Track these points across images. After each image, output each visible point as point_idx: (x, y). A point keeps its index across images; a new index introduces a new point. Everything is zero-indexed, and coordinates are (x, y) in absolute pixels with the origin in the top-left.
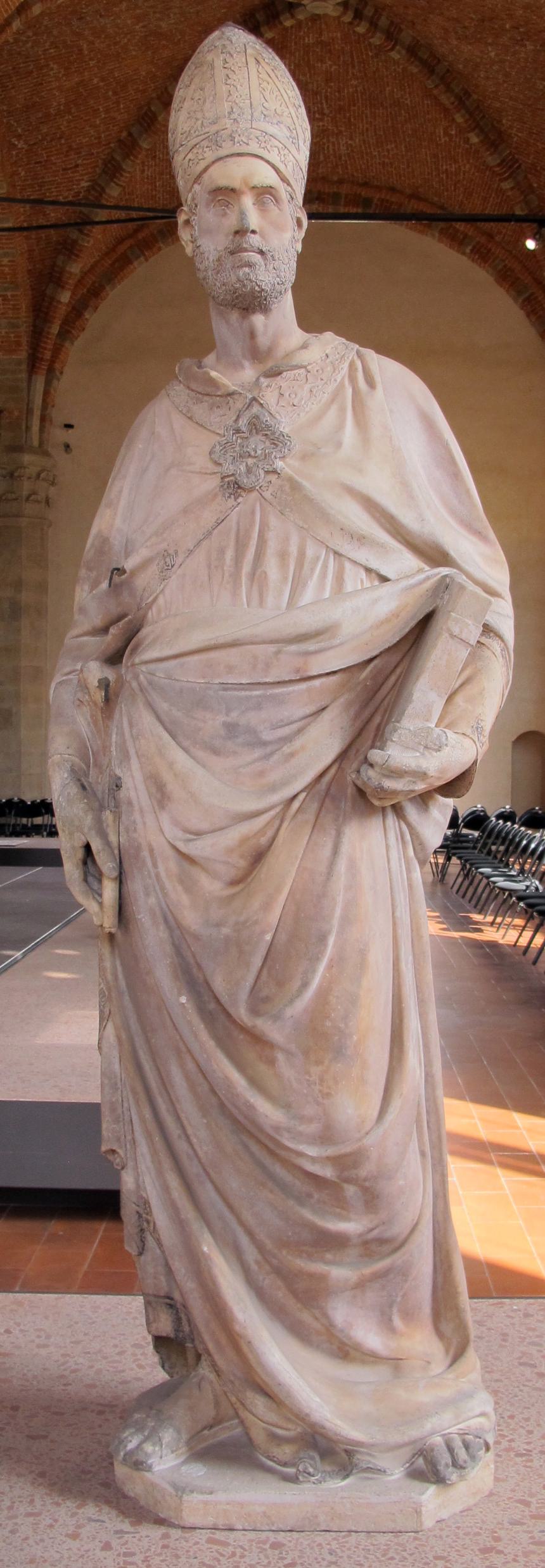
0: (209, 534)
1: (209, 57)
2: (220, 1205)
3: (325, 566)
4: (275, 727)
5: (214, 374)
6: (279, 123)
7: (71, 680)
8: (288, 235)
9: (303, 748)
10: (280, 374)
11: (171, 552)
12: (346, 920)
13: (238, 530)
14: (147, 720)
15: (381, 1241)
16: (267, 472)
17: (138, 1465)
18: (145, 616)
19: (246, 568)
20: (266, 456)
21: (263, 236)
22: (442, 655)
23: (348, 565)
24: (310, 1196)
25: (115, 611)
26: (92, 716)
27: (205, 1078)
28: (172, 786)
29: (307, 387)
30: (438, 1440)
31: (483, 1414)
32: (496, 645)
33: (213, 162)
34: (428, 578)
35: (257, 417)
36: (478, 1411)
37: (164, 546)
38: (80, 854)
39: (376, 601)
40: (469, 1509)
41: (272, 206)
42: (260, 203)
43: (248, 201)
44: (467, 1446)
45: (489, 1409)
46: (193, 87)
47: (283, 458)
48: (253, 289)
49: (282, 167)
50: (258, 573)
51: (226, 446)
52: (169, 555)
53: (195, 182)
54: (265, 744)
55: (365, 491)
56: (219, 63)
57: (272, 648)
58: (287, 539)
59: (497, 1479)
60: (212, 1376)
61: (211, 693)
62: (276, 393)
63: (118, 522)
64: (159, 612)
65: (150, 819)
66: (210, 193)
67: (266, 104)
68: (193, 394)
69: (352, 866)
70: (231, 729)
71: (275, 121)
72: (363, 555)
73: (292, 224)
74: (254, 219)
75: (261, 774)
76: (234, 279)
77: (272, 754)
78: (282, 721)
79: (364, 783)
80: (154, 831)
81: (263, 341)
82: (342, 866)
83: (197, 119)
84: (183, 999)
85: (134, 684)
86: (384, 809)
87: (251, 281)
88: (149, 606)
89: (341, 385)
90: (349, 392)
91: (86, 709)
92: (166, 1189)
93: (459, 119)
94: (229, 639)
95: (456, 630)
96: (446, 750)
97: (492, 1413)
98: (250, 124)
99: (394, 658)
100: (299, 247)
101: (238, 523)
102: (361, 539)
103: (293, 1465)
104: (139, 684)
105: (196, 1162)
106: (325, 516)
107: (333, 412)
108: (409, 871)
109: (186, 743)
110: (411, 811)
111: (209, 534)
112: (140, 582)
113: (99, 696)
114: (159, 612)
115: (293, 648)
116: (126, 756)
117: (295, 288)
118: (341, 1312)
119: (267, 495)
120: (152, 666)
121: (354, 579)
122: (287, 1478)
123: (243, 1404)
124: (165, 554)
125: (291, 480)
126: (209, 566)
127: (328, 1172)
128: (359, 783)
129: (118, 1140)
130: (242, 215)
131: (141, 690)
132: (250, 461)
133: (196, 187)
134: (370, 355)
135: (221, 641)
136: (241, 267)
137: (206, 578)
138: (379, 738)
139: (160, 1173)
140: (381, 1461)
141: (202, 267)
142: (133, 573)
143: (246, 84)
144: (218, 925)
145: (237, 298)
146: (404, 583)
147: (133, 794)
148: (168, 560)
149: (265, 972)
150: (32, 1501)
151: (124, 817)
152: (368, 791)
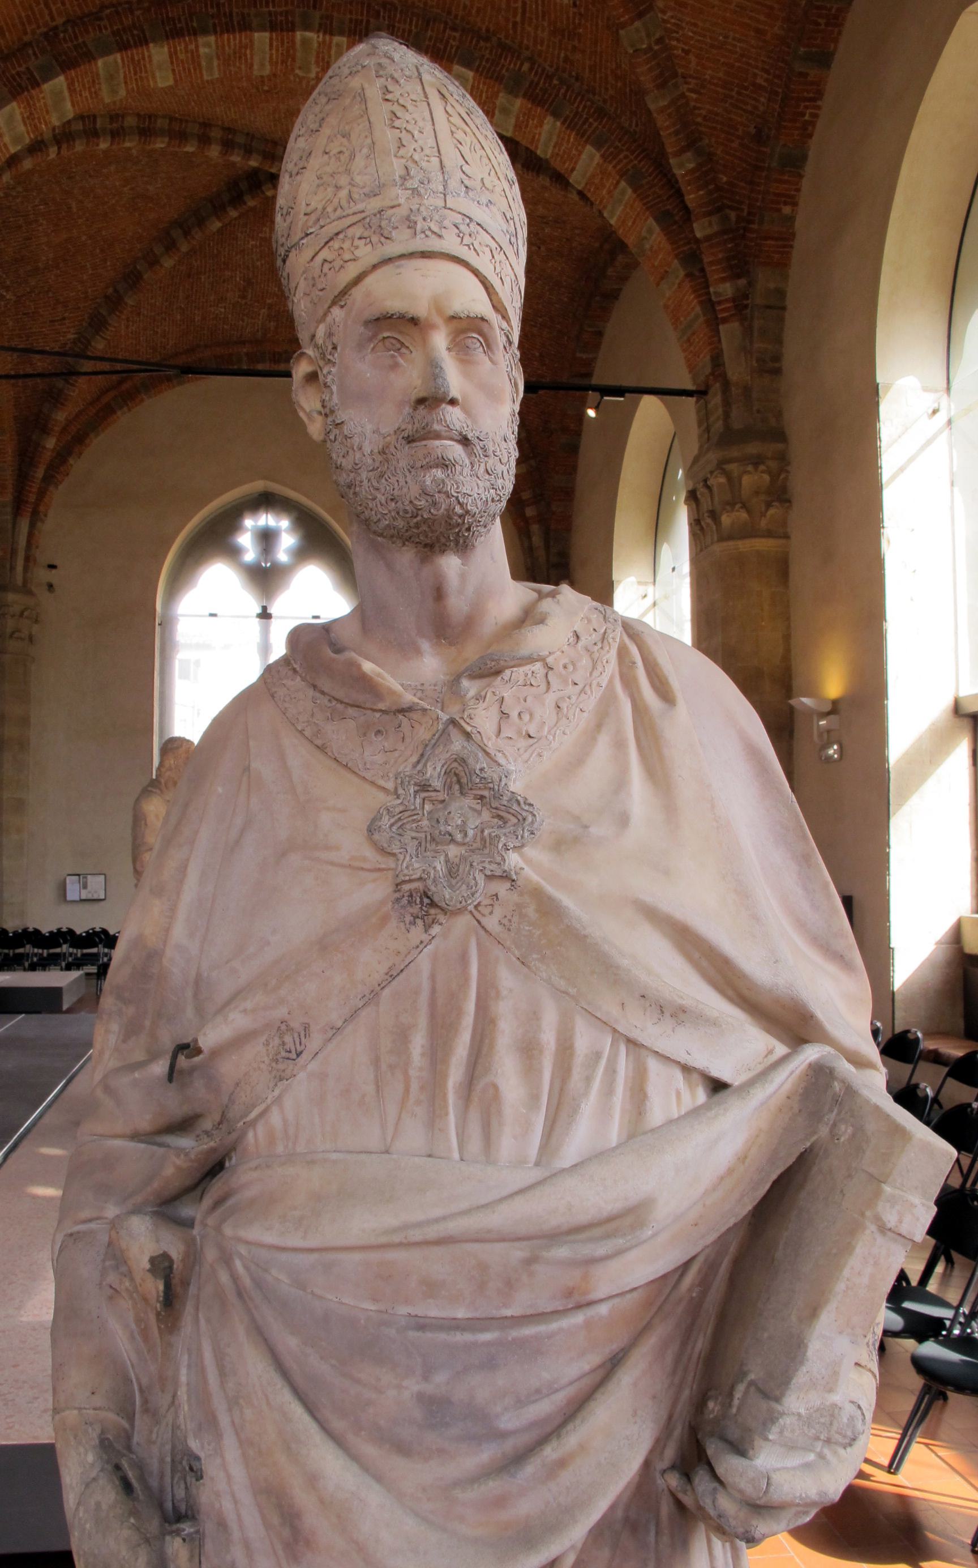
0: (372, 997)
1: (355, 83)
3: (611, 1071)
4: (521, 1403)
7: (91, 1232)
9: (582, 1448)
10: (498, 672)
11: (295, 1024)
13: (433, 991)
16: (490, 878)
20: (486, 844)
21: (467, 411)
23: (653, 1065)
25: (174, 1105)
26: (138, 1321)
28: (313, 1520)
29: (550, 698)
33: (375, 267)
37: (281, 1012)
41: (479, 355)
42: (459, 346)
46: (326, 131)
48: (450, 510)
50: (480, 1086)
52: (289, 1029)
53: (334, 303)
54: (503, 1435)
55: (679, 914)
56: (373, 92)
57: (518, 1253)
58: (534, 1016)
61: (392, 1332)
62: (494, 713)
63: (179, 932)
64: (272, 1140)
66: (367, 323)
67: (465, 168)
68: (325, 700)
70: (436, 1409)
71: (484, 200)
73: (508, 388)
75: (500, 1502)
76: (414, 490)
78: (538, 1391)
81: (457, 604)
83: (338, 188)
85: (224, 1277)
87: (448, 495)
91: (125, 1304)
95: (891, 1219)
101: (433, 977)
102: (678, 1014)
104: (235, 1278)
106: (609, 971)
109: (338, 1425)
111: (372, 997)
112: (229, 1069)
114: (272, 1140)
116: (210, 1423)
119: (492, 923)
124: (283, 1027)
125: (538, 894)
126: (376, 1062)
130: (433, 369)
131: (240, 1294)
132: (453, 851)
133: (337, 312)
136: (428, 467)
137: (370, 1089)
141: (346, 463)
142: (216, 1053)
143: (429, 127)
145: (417, 526)
147: (227, 1505)
148: (288, 1039)
151: (209, 1546)
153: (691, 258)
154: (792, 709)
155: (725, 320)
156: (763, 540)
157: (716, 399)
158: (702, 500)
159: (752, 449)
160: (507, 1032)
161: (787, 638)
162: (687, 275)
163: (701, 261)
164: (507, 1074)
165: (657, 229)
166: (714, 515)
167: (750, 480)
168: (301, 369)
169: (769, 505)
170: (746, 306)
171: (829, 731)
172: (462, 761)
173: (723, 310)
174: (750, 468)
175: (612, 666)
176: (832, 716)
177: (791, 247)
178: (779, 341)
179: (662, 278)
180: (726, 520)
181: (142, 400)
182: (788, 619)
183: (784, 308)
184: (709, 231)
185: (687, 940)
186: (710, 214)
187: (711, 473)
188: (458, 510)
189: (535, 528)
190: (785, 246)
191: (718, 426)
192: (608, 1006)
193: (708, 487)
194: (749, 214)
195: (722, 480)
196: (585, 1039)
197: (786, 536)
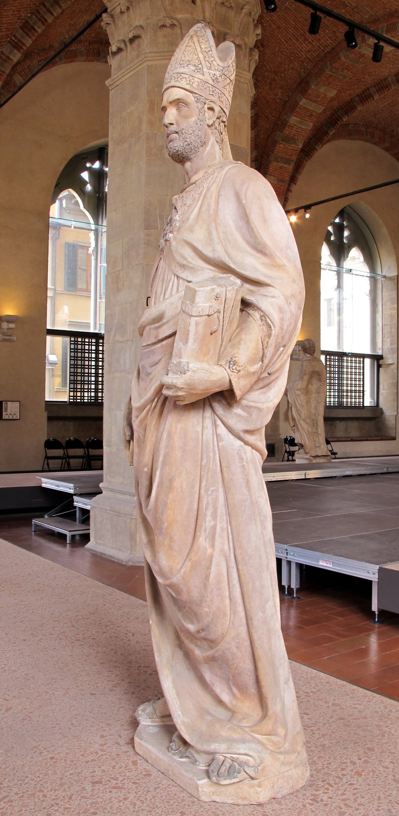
9: (155, 375)
12: (164, 463)
23: (181, 281)
49: (188, 87)
96: (189, 373)
188: (174, 151)
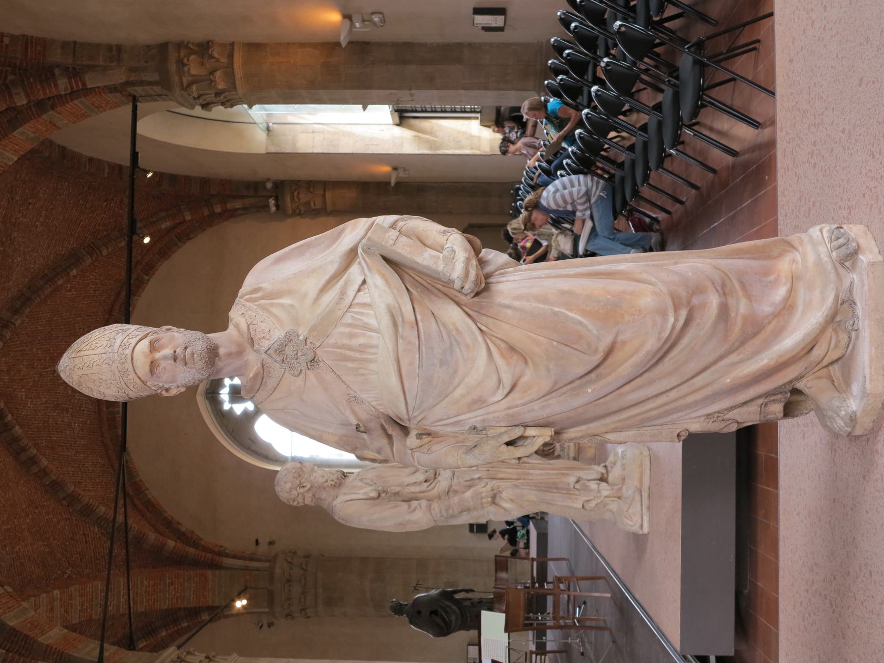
1: (75, 377)
2: (705, 374)
3: (357, 313)
5: (251, 375)
6: (114, 339)
8: (176, 334)
14: (439, 412)
15: (723, 285)
16: (306, 344)
17: (853, 419)
18: (383, 414)
19: (358, 355)
21: (177, 347)
22: (404, 249)
23: (356, 301)
24: (698, 324)
25: (380, 431)
27: (634, 379)
29: (260, 324)
30: (834, 254)
31: (821, 231)
32: (400, 224)
34: (364, 259)
35: (276, 351)
36: (819, 233)
38: (510, 448)
39: (376, 286)
40: (874, 237)
43: (158, 355)
44: (838, 238)
45: (818, 227)
46: (92, 386)
47: (298, 336)
49: (139, 337)
51: (291, 368)
54: (451, 345)
56: (80, 372)
57: (400, 341)
59: (861, 223)
60: (804, 381)
62: (263, 341)
64: (380, 405)
65: (492, 408)
69: (518, 298)
70: (442, 363)
72: (351, 293)
74: (168, 351)
75: (467, 346)
76: (200, 363)
77: (456, 341)
79: (472, 292)
80: (499, 407)
81: (233, 349)
82: (516, 304)
84: (590, 390)
86: (487, 284)
88: (377, 410)
89: (259, 306)
90: (262, 301)
92: (696, 403)
93: (61, 282)
94: (395, 364)
95: (391, 242)
97: (821, 225)
98: (109, 359)
99: (406, 277)
100: (182, 330)
102: (343, 293)
103: (850, 333)
104: (419, 415)
105: (681, 387)
107: (274, 310)
108: (521, 270)
110: (489, 269)
112: (364, 416)
113: (426, 439)
115: (400, 329)
117: (207, 331)
118: (766, 309)
119: (318, 344)
120: (410, 408)
121: (363, 297)
122: (857, 337)
123: (819, 363)
124: (349, 401)
125: (310, 331)
127: (683, 314)
128: (472, 295)
129: (671, 432)
130: (165, 358)
132: (299, 354)
133: (148, 384)
134: (242, 291)
135: (396, 368)
138: (449, 283)
139: (687, 407)
140: (846, 283)
142: (359, 420)
144: (549, 371)
146: (366, 271)
147: (479, 419)
149: (574, 346)
150: (876, 480)
151: (491, 424)
152: (477, 290)
153: (41, 106)
154: (350, 43)
155: (84, 84)
156: (235, 61)
157: (139, 90)
158: (208, 100)
159: (173, 67)
160: (346, 341)
161: (302, 45)
162: (53, 109)
163: (42, 100)
164: (356, 342)
165: (21, 129)
166: (218, 94)
167: (194, 69)
168: (164, 394)
169: (211, 57)
170: (74, 69)
171: (364, 21)
172: (276, 351)
173: (77, 85)
174: (186, 69)
175: (251, 304)
176: (354, 19)
177: (32, 37)
178: (98, 46)
179: (55, 125)
180: (221, 86)
181: (141, 480)
182: (288, 44)
183: (75, 43)
184: (23, 95)
185: (323, 290)
186: (11, 95)
187: (189, 95)
189: (229, 206)
190: (32, 43)
191: (157, 89)
192: (340, 313)
193: (199, 97)
194: (9, 66)
195: (194, 88)
196: (348, 319)
197: (232, 44)
